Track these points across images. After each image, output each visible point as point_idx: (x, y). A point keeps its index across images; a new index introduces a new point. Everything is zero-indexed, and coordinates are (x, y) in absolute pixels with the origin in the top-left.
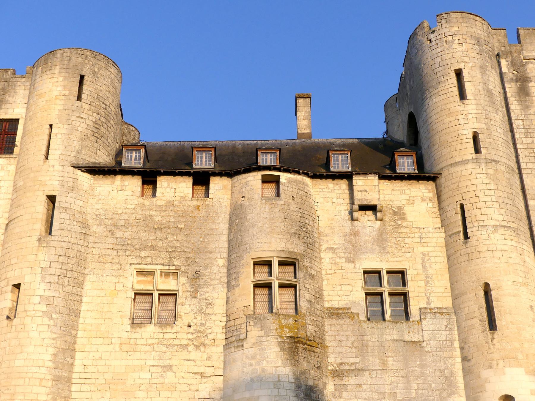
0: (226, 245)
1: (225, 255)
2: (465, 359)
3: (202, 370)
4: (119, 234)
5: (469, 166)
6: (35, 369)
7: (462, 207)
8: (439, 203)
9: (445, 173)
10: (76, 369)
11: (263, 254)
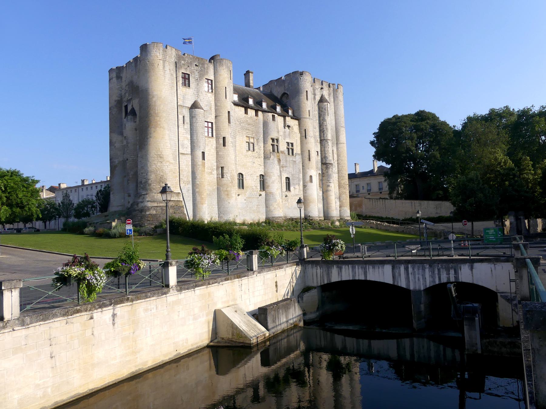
0: (262, 131)
1: (263, 134)
2: (303, 166)
3: (260, 164)
4: (242, 125)
5: (308, 119)
6: (232, 161)
7: (305, 130)
8: (299, 127)
9: (302, 119)
10: (237, 161)
11: (273, 137)
